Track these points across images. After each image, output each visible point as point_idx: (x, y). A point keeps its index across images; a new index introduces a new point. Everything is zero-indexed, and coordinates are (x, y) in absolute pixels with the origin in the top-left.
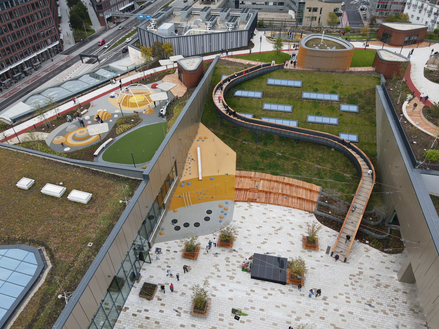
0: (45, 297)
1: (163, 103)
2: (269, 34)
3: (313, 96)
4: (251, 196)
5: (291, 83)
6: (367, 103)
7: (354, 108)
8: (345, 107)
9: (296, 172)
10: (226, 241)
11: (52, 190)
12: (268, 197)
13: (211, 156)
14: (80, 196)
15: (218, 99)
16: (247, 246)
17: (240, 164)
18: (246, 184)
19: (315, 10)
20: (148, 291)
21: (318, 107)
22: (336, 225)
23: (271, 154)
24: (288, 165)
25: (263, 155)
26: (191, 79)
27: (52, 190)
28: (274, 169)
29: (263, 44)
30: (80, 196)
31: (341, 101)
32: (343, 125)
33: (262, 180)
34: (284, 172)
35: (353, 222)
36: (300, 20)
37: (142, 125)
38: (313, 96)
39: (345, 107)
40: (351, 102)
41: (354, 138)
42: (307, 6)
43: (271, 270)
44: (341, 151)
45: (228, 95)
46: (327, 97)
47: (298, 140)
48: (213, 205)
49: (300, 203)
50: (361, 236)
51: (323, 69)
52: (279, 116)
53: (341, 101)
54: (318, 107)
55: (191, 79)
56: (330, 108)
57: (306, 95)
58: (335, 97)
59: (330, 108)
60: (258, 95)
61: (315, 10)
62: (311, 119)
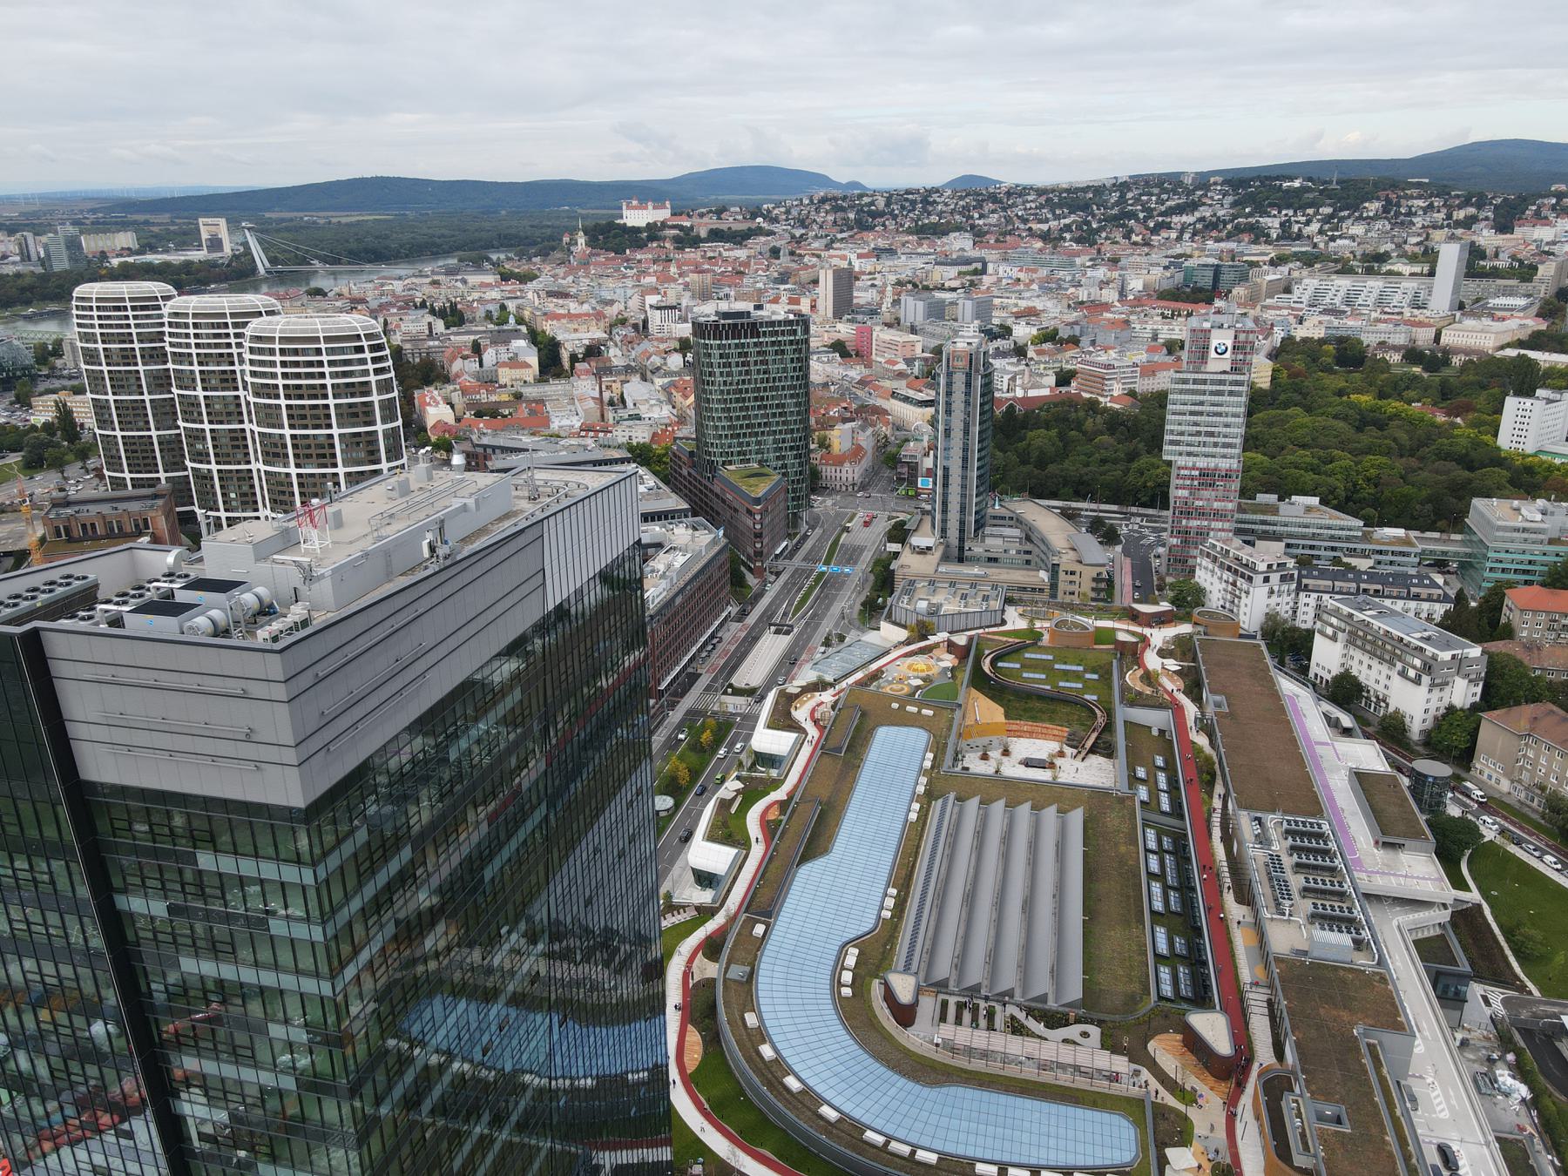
1: (946, 669)
2: (1020, 609)
3: (1063, 667)
4: (1019, 734)
6: (1105, 674)
7: (1095, 677)
8: (1088, 676)
9: (1051, 720)
10: (1006, 753)
13: (985, 710)
15: (986, 667)
17: (1007, 717)
19: (1073, 573)
21: (1067, 675)
23: (1031, 709)
25: (1025, 710)
26: (962, 653)
28: (1034, 719)
29: (1015, 620)
31: (1085, 671)
32: (1086, 689)
33: (1026, 726)
34: (1043, 721)
36: (1054, 586)
38: (1063, 667)
39: (1088, 676)
42: (1062, 568)
44: (1086, 706)
45: (993, 663)
46: (1074, 668)
47: (1052, 699)
49: (1055, 737)
51: (1073, 646)
52: (1035, 679)
53: (1085, 671)
54: (1067, 675)
55: (962, 653)
56: (1077, 676)
59: (1077, 676)
61: (1073, 573)
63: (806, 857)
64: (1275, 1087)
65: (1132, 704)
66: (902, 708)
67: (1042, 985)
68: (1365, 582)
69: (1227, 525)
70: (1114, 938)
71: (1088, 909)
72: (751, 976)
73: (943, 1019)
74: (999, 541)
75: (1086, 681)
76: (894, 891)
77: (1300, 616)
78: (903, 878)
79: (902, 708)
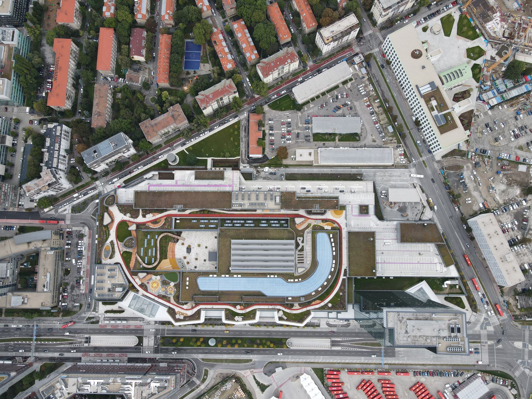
0: (202, 275)
5: (142, 250)
7: (149, 236)
10: (185, 258)
11: (187, 283)
12: (173, 252)
14: (188, 279)
16: (186, 254)
18: (171, 256)
20: (196, 267)
22: (178, 240)
24: (164, 249)
27: (187, 283)
30: (188, 279)
31: (147, 238)
35: (179, 237)
37: (166, 279)
40: (147, 236)
41: (157, 236)
43: (189, 250)
48: (177, 262)
50: (180, 236)
53: (147, 238)
57: (146, 246)
58: (146, 240)
60: (146, 258)
62: (152, 245)
63: (263, 295)
64: (310, 213)
65: (171, 227)
66: (187, 286)
67: (293, 247)
68: (54, 148)
69: (4, 185)
70: (272, 234)
71: (265, 239)
72: (302, 296)
73: (303, 263)
74: (9, 271)
75: (151, 239)
76: (268, 276)
77: (64, 169)
78: (264, 275)
79: (187, 286)
